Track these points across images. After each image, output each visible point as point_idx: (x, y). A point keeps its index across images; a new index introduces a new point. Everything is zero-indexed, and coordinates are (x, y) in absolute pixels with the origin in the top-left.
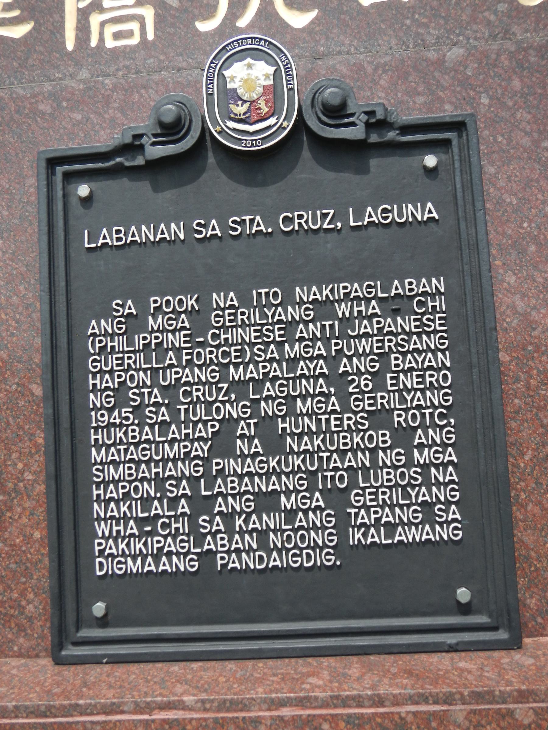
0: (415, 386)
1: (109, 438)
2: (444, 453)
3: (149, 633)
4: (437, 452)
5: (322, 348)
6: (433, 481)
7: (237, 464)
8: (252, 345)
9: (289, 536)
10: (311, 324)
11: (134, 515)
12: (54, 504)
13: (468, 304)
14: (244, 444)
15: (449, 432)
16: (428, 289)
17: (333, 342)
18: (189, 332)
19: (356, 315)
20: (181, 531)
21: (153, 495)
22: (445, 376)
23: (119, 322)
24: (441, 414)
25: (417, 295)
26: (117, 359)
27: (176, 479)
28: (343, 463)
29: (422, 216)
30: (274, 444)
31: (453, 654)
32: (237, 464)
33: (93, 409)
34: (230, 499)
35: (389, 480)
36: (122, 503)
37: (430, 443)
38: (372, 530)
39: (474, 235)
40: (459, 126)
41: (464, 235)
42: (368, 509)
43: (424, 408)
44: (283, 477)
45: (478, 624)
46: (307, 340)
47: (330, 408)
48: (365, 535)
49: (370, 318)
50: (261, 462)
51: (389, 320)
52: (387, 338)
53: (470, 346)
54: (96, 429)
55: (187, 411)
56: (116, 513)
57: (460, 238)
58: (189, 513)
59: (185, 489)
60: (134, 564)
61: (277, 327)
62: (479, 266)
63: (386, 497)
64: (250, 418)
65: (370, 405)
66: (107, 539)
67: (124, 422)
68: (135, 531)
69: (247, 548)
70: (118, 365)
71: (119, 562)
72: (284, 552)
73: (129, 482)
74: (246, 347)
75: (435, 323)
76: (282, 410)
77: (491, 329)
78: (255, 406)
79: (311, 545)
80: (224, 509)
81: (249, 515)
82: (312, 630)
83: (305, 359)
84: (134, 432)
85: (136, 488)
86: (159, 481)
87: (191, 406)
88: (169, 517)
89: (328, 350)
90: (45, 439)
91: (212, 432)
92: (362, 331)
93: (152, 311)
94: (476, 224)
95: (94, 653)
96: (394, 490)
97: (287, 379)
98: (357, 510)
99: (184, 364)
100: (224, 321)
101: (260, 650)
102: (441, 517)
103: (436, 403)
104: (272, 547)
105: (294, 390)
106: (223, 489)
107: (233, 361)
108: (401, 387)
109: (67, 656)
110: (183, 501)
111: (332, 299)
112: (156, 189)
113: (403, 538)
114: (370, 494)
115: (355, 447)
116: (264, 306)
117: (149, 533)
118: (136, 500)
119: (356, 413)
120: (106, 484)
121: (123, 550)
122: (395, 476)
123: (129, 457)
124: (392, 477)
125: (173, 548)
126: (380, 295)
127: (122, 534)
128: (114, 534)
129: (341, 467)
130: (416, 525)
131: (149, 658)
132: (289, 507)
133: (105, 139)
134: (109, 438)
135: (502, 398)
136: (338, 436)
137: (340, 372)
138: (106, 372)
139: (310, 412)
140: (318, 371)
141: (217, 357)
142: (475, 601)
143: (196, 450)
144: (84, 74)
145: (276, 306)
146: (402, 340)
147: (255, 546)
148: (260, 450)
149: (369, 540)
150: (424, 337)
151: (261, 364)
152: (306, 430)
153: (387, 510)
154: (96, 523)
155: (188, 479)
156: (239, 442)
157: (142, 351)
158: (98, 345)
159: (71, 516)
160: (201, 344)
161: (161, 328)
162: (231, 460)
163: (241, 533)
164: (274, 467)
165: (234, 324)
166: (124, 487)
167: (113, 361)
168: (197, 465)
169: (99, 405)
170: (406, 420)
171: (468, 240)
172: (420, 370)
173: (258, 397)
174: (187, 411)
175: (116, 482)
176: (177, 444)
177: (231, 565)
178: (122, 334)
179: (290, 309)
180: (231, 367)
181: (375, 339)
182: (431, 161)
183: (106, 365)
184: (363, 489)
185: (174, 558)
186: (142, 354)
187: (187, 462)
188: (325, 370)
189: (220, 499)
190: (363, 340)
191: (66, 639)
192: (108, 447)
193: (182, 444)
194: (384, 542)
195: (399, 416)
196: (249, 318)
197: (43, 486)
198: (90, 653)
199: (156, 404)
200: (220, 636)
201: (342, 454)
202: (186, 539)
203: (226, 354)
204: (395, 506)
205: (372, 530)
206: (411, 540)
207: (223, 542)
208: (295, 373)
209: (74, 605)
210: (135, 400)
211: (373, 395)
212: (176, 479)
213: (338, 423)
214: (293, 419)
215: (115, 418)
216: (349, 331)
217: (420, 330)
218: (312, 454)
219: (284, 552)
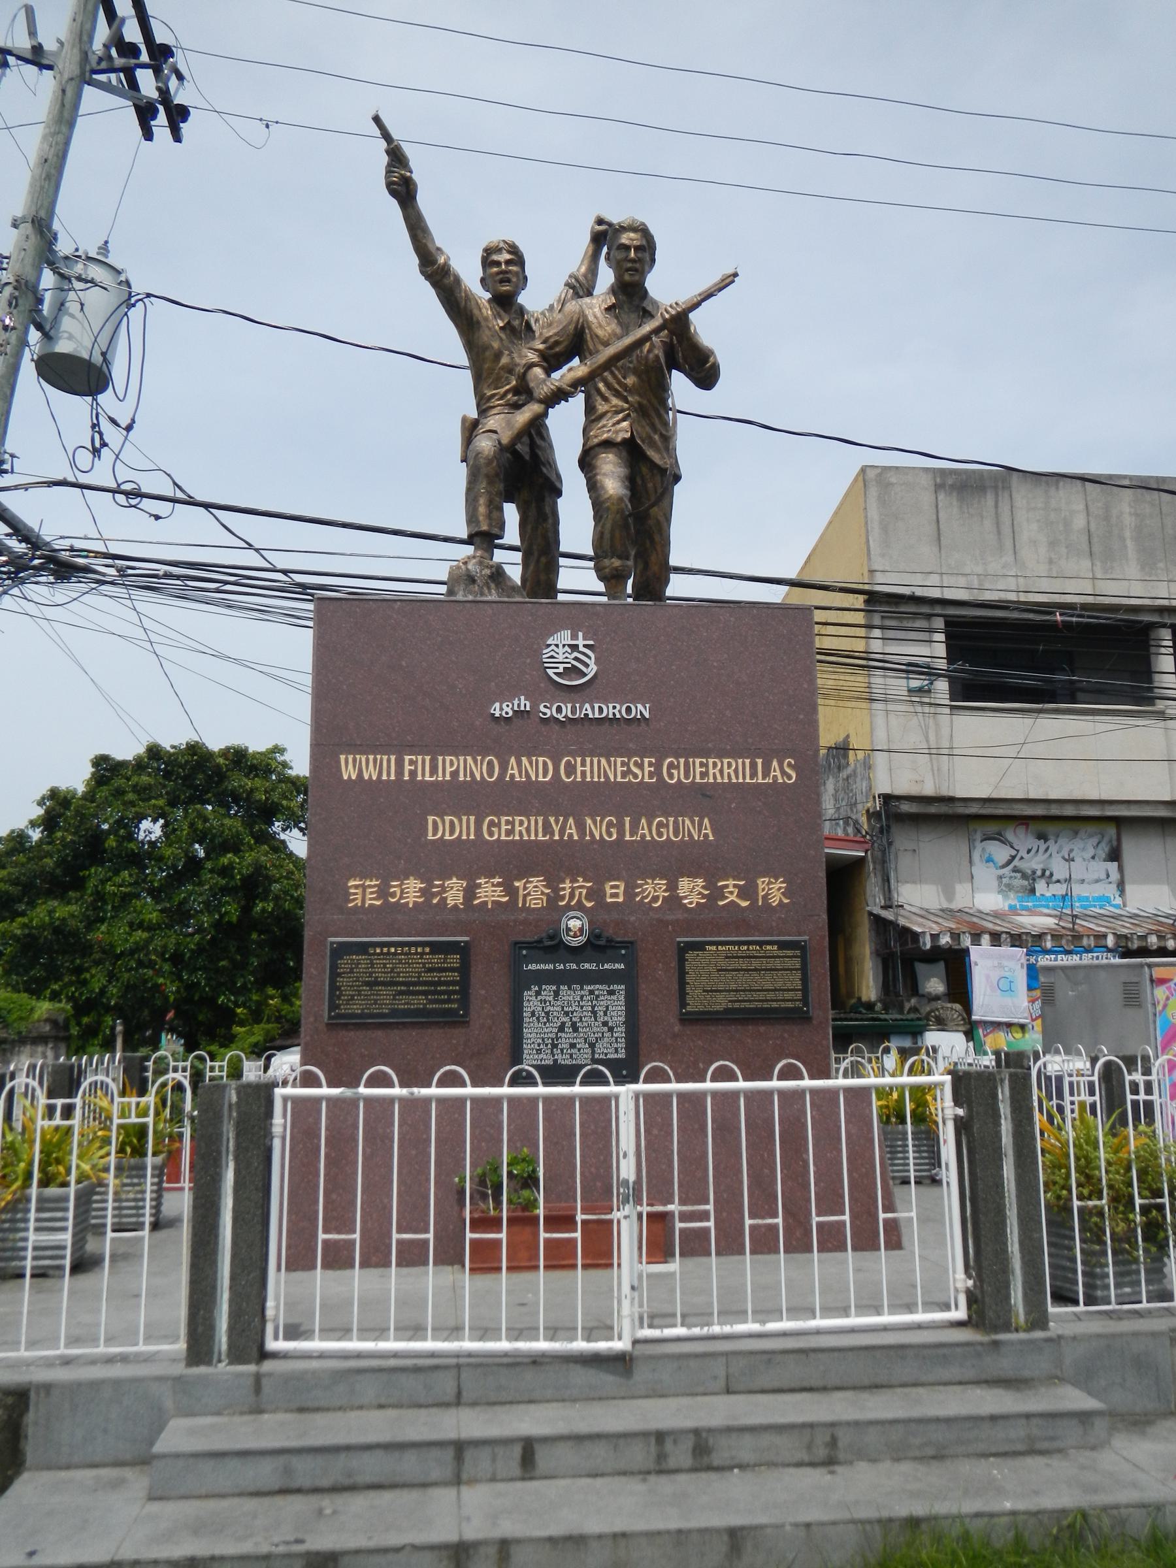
30: (575, 1029)
182: (623, 952)
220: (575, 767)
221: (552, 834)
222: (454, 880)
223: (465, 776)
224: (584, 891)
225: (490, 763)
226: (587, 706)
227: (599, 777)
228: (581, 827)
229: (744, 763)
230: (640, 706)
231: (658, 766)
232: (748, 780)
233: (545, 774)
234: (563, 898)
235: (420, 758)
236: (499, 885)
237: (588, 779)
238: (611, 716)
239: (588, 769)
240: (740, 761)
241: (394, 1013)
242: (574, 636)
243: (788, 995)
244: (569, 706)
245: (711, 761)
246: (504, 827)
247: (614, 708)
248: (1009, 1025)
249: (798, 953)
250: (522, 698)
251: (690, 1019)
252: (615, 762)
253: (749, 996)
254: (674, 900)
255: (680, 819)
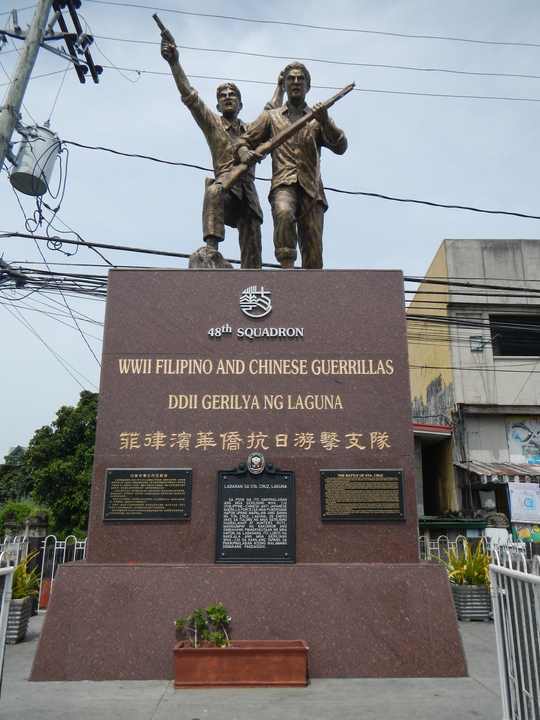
30: (256, 526)
79: (261, 544)
86: (235, 532)
201: (267, 529)
220: (258, 365)
221: (244, 405)
222: (184, 433)
223: (192, 371)
224: (263, 440)
225: (208, 364)
226: (266, 329)
227: (273, 371)
228: (261, 401)
229: (361, 363)
230: (297, 329)
231: (309, 365)
232: (364, 373)
233: (240, 370)
234: (249, 444)
235: (166, 361)
236: (211, 436)
237: (266, 373)
238: (280, 335)
239: (266, 366)
240: (359, 361)
241: (144, 515)
242: (259, 289)
243: (390, 506)
244: (255, 329)
245: (341, 361)
246: (214, 402)
247: (282, 330)
248: (532, 525)
249: (396, 479)
250: (227, 325)
251: (327, 520)
252: (283, 362)
253: (365, 506)
254: (318, 446)
255: (322, 396)
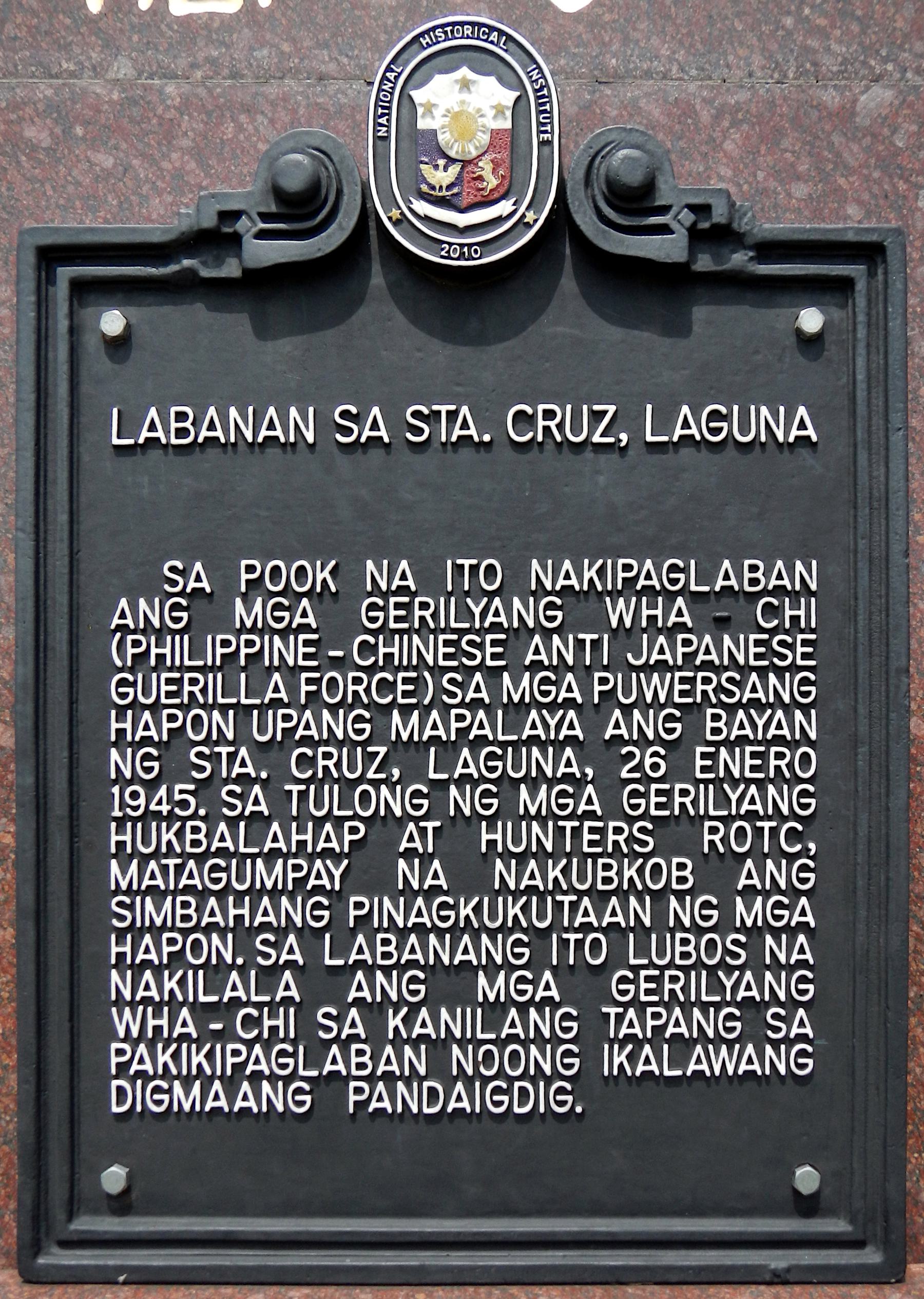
0: (748, 774)
1: (146, 842)
2: (790, 908)
3: (211, 1228)
4: (778, 905)
5: (574, 686)
6: (768, 961)
7: (397, 908)
8: (438, 671)
9: (489, 1053)
10: (555, 637)
11: (191, 999)
12: (32, 967)
13: (860, 617)
14: (412, 869)
15: (804, 868)
16: (786, 582)
17: (597, 675)
18: (315, 637)
19: (644, 624)
20: (282, 1034)
21: (229, 960)
22: (805, 757)
23: (175, 607)
24: (792, 830)
25: (765, 592)
26: (169, 681)
27: (276, 930)
28: (600, 916)
29: (787, 433)
30: (471, 872)
31: (779, 1289)
32: (397, 908)
33: (115, 782)
34: (380, 976)
35: (685, 955)
36: (166, 973)
37: (768, 887)
38: (647, 1049)
39: (882, 479)
40: (870, 252)
41: (863, 478)
42: (641, 1008)
43: (761, 819)
44: (484, 938)
45: (830, 1234)
46: (546, 669)
47: (583, 807)
48: (632, 1058)
49: (671, 632)
50: (443, 906)
51: (707, 639)
52: (700, 675)
53: (856, 700)
54: (121, 822)
55: (303, 795)
56: (154, 993)
57: (855, 484)
58: (298, 999)
59: (292, 950)
60: (187, 1095)
61: (489, 637)
62: (887, 543)
63: (677, 987)
64: (425, 818)
65: (659, 806)
66: (136, 1043)
67: (177, 811)
68: (191, 1030)
69: (407, 1073)
70: (169, 695)
71: (157, 1090)
72: (477, 1084)
73: (182, 931)
74: (426, 674)
75: (794, 653)
76: (490, 806)
77: (899, 671)
78: (437, 794)
79: (526, 1069)
80: (366, 994)
81: (414, 1009)
82: (521, 1234)
83: (540, 706)
84: (196, 834)
85: (196, 944)
86: (243, 933)
87: (312, 787)
88: (259, 1006)
89: (586, 691)
90: (17, 836)
91: (351, 842)
92: (655, 657)
93: (243, 589)
94: (887, 457)
95: (101, 1263)
96: (693, 973)
97: (504, 745)
98: (621, 1010)
99: (303, 701)
100: (386, 619)
101: (421, 1269)
102: (777, 1030)
103: (785, 810)
104: (455, 1072)
105: (516, 767)
106: (367, 956)
107: (401, 701)
108: (722, 775)
109: (47, 1267)
110: (287, 975)
111: (600, 588)
112: (263, 331)
113: (704, 1067)
114: (648, 979)
115: (625, 887)
116: (467, 594)
117: (218, 1036)
118: (196, 968)
119: (631, 820)
120: (137, 932)
121: (165, 1065)
122: (697, 948)
123: (184, 881)
124: (690, 948)
125: (263, 1067)
126: (693, 588)
127: (166, 1034)
128: (150, 1035)
129: (596, 924)
130: (730, 1044)
131: (207, 1276)
132: (492, 997)
133: (161, 215)
134: (146, 842)
135: (908, 807)
136: (595, 864)
137: (607, 737)
138: (145, 707)
139: (544, 813)
140: (564, 732)
141: (367, 690)
142: (827, 1192)
143: (319, 876)
144: (123, 68)
145: (491, 595)
146: (730, 680)
147: (422, 1071)
148: (442, 882)
149: (641, 1068)
150: (772, 679)
151: (454, 712)
152: (534, 849)
153: (677, 1012)
154: (114, 1010)
155: (300, 932)
156: (402, 864)
157: (220, 668)
158: (131, 651)
159: (66, 994)
160: (336, 663)
161: (260, 625)
162: (386, 899)
163: (398, 1042)
164: (467, 917)
165: (405, 626)
166: (172, 942)
167: (160, 685)
168: (317, 906)
169: (128, 774)
170: (725, 840)
171: (871, 489)
172: (759, 743)
173: (445, 776)
174: (303, 795)
175: (156, 931)
176: (280, 861)
177: (374, 1105)
178: (181, 632)
179: (517, 603)
180: (395, 713)
181: (678, 674)
182: (811, 320)
183: (146, 693)
184: (635, 969)
185: (266, 1087)
186: (219, 676)
187: (299, 899)
188: (578, 732)
189: (360, 975)
190: (656, 675)
191: (47, 1234)
192: (145, 859)
193: (291, 862)
194: (667, 1073)
195: (714, 830)
196: (435, 616)
197: (11, 930)
198: (93, 1262)
199: (242, 779)
200: (346, 1238)
202: (290, 1049)
203: (386, 686)
204: (693, 1004)
205: (647, 1049)
206: (717, 1072)
207: (361, 1060)
208: (520, 734)
209: (66, 1169)
210: (202, 769)
211: (666, 786)
212: (276, 930)
213: (597, 837)
214: (509, 824)
215: (160, 803)
216: (629, 656)
217: (766, 663)
218: (542, 896)
219: (477, 1084)
